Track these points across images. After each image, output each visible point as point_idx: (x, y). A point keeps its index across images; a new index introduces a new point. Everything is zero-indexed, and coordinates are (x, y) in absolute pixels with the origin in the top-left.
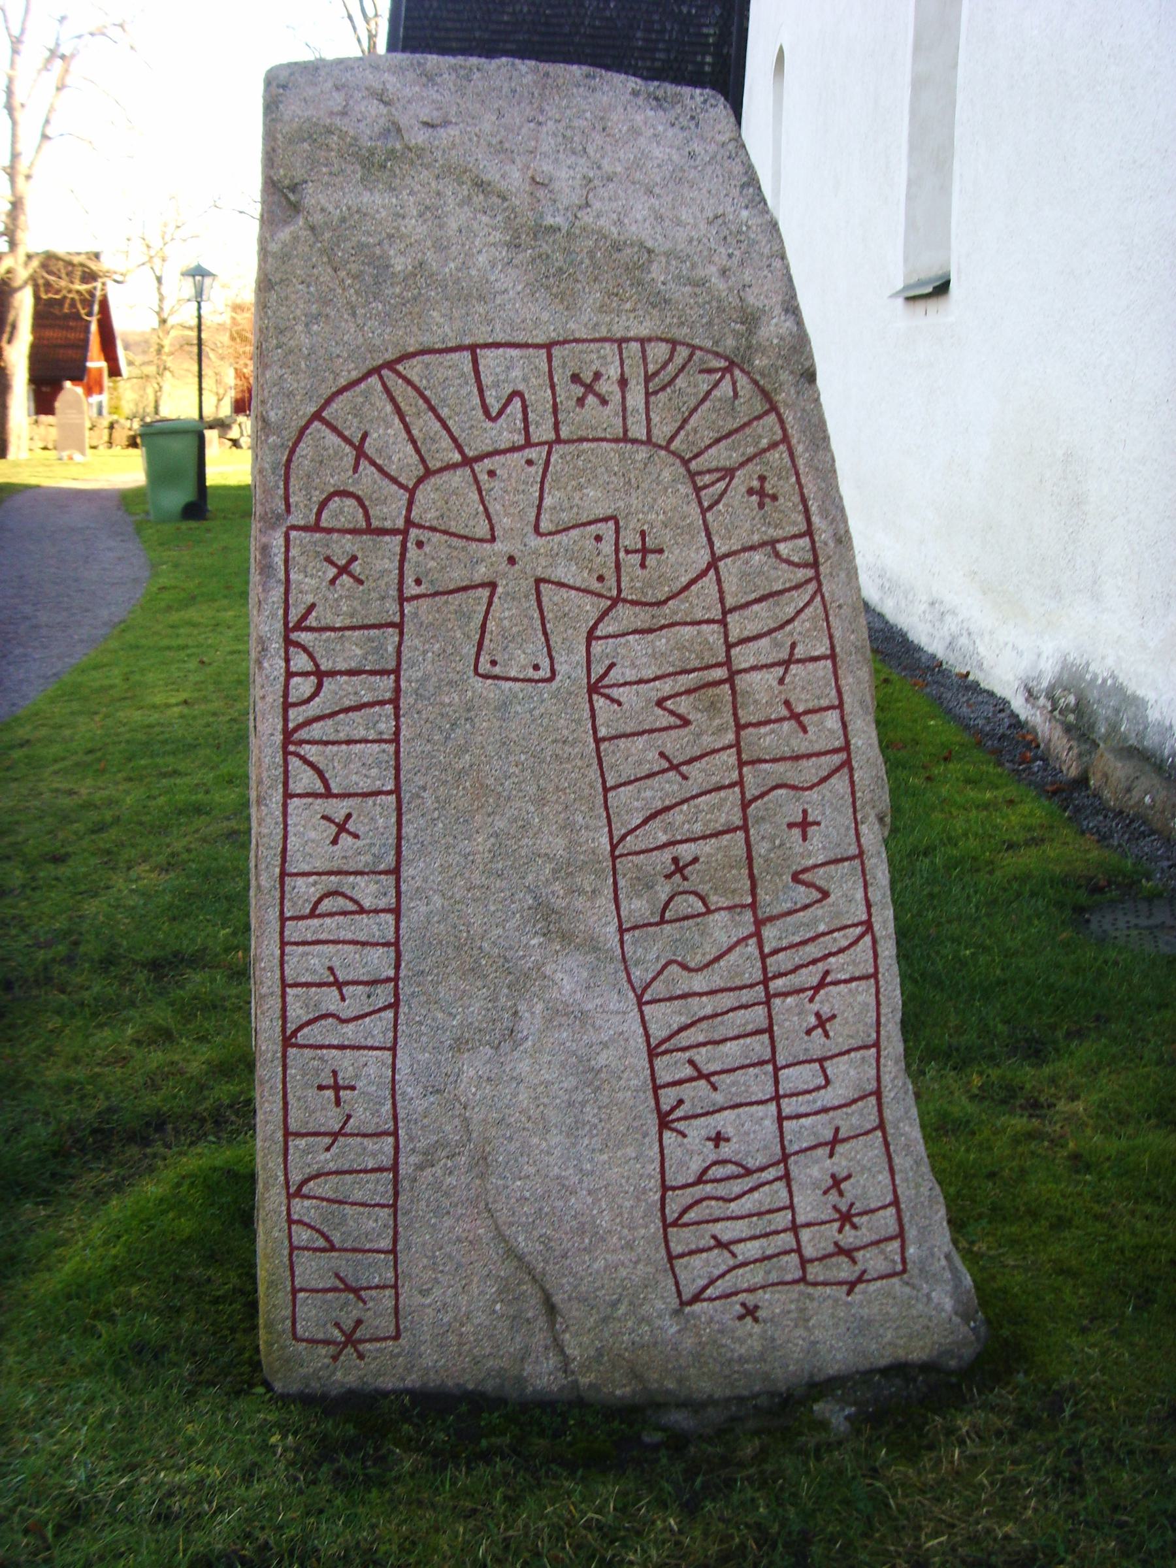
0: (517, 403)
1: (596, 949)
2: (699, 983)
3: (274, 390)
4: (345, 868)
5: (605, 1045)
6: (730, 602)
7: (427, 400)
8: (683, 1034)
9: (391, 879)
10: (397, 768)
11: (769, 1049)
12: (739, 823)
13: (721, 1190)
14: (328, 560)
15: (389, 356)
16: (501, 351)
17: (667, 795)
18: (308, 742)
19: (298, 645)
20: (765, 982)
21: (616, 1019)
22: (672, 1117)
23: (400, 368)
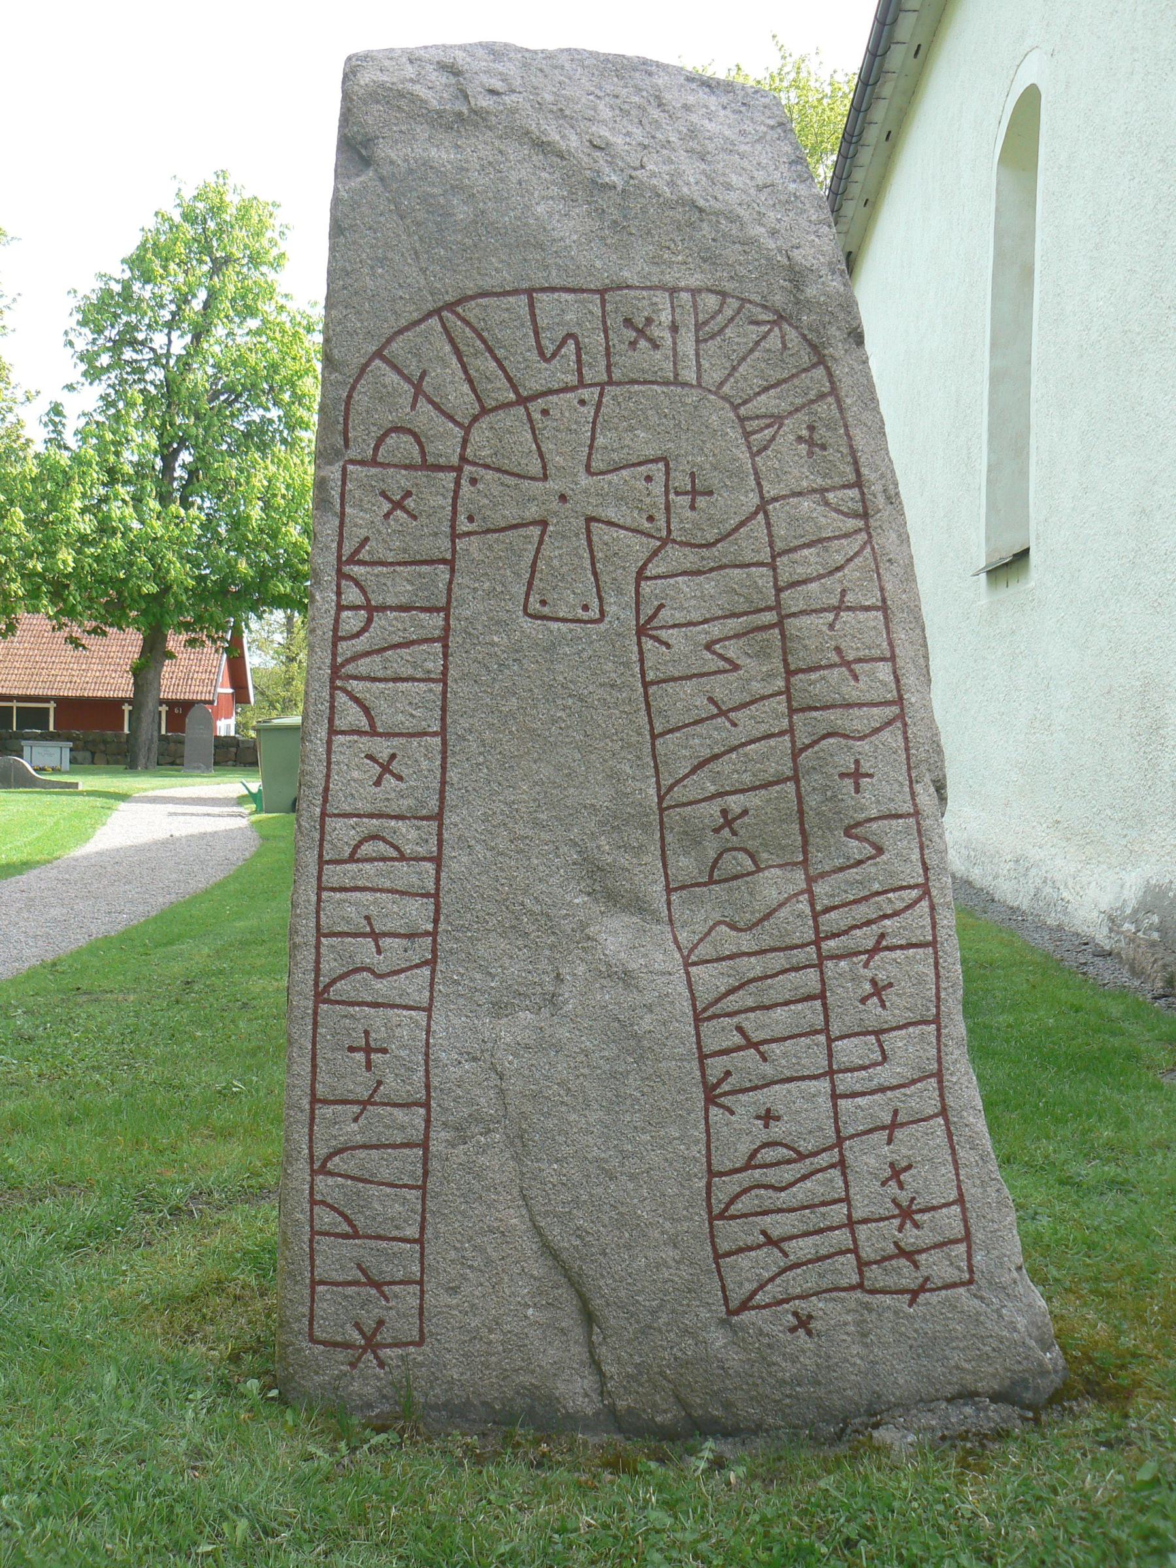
0: (571, 344)
1: (641, 910)
2: (746, 942)
3: (338, 329)
4: (389, 811)
5: (649, 1008)
6: (780, 545)
7: (484, 341)
8: (731, 998)
9: (434, 824)
10: (444, 709)
11: (822, 1017)
12: (790, 773)
13: (772, 1176)
14: (383, 494)
15: (449, 298)
16: (556, 295)
17: (716, 743)
18: (356, 678)
19: (349, 577)
20: (817, 942)
21: (661, 980)
22: (718, 1091)
23: (459, 310)
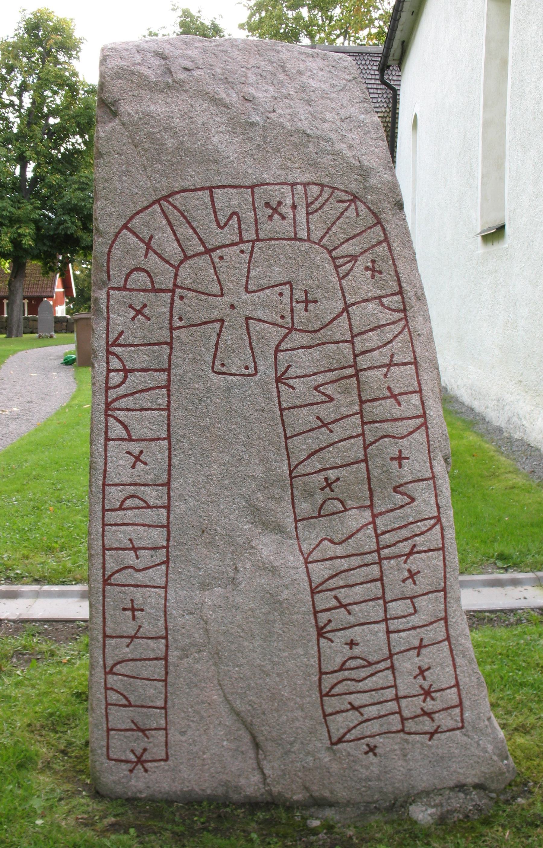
0: (235, 218)
1: (281, 532)
2: (339, 550)
4: (140, 482)
6: (356, 330)
7: (185, 217)
8: (331, 581)
9: (165, 488)
10: (169, 425)
11: (381, 591)
12: (362, 458)
13: (354, 674)
14: (131, 306)
15: (164, 193)
16: (226, 190)
18: (119, 409)
20: (378, 551)
21: (292, 572)
22: (325, 630)
23: (170, 199)
